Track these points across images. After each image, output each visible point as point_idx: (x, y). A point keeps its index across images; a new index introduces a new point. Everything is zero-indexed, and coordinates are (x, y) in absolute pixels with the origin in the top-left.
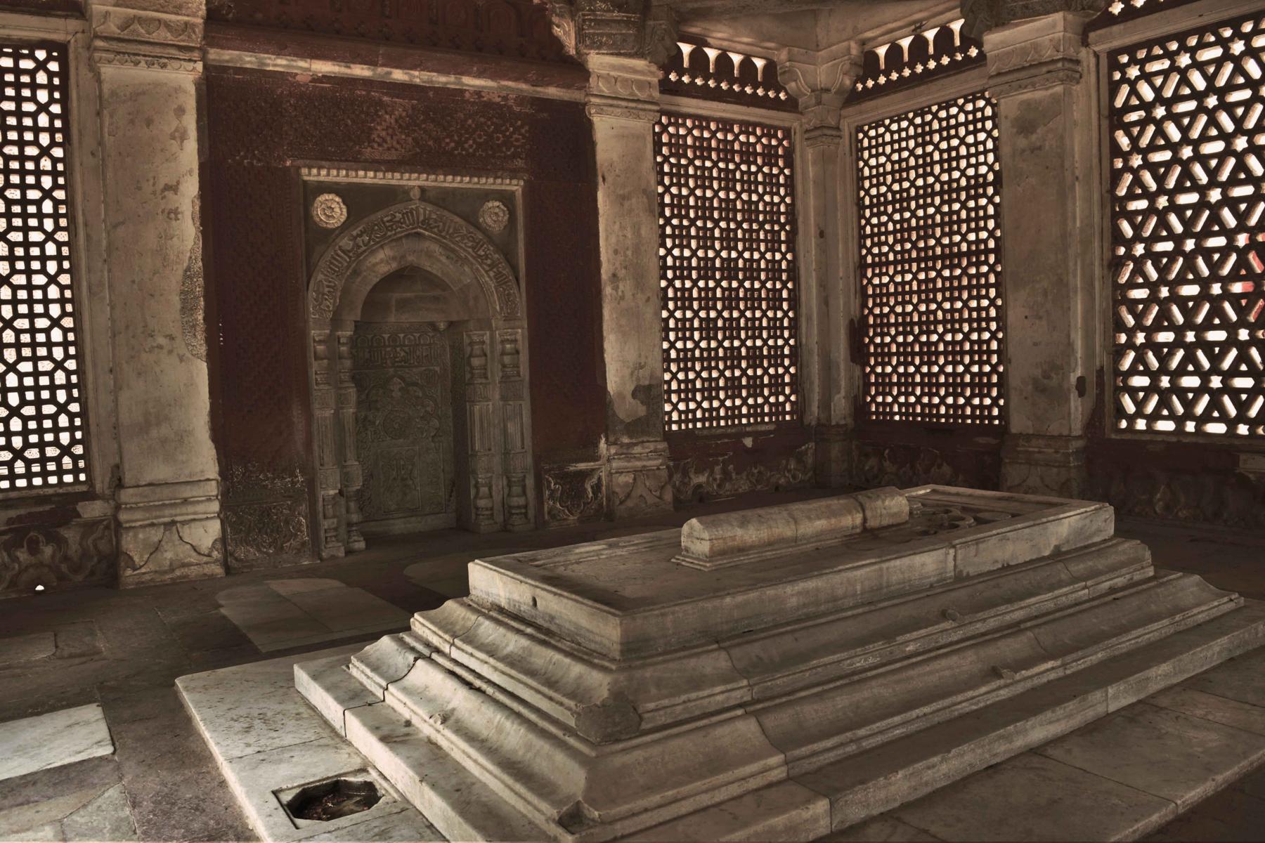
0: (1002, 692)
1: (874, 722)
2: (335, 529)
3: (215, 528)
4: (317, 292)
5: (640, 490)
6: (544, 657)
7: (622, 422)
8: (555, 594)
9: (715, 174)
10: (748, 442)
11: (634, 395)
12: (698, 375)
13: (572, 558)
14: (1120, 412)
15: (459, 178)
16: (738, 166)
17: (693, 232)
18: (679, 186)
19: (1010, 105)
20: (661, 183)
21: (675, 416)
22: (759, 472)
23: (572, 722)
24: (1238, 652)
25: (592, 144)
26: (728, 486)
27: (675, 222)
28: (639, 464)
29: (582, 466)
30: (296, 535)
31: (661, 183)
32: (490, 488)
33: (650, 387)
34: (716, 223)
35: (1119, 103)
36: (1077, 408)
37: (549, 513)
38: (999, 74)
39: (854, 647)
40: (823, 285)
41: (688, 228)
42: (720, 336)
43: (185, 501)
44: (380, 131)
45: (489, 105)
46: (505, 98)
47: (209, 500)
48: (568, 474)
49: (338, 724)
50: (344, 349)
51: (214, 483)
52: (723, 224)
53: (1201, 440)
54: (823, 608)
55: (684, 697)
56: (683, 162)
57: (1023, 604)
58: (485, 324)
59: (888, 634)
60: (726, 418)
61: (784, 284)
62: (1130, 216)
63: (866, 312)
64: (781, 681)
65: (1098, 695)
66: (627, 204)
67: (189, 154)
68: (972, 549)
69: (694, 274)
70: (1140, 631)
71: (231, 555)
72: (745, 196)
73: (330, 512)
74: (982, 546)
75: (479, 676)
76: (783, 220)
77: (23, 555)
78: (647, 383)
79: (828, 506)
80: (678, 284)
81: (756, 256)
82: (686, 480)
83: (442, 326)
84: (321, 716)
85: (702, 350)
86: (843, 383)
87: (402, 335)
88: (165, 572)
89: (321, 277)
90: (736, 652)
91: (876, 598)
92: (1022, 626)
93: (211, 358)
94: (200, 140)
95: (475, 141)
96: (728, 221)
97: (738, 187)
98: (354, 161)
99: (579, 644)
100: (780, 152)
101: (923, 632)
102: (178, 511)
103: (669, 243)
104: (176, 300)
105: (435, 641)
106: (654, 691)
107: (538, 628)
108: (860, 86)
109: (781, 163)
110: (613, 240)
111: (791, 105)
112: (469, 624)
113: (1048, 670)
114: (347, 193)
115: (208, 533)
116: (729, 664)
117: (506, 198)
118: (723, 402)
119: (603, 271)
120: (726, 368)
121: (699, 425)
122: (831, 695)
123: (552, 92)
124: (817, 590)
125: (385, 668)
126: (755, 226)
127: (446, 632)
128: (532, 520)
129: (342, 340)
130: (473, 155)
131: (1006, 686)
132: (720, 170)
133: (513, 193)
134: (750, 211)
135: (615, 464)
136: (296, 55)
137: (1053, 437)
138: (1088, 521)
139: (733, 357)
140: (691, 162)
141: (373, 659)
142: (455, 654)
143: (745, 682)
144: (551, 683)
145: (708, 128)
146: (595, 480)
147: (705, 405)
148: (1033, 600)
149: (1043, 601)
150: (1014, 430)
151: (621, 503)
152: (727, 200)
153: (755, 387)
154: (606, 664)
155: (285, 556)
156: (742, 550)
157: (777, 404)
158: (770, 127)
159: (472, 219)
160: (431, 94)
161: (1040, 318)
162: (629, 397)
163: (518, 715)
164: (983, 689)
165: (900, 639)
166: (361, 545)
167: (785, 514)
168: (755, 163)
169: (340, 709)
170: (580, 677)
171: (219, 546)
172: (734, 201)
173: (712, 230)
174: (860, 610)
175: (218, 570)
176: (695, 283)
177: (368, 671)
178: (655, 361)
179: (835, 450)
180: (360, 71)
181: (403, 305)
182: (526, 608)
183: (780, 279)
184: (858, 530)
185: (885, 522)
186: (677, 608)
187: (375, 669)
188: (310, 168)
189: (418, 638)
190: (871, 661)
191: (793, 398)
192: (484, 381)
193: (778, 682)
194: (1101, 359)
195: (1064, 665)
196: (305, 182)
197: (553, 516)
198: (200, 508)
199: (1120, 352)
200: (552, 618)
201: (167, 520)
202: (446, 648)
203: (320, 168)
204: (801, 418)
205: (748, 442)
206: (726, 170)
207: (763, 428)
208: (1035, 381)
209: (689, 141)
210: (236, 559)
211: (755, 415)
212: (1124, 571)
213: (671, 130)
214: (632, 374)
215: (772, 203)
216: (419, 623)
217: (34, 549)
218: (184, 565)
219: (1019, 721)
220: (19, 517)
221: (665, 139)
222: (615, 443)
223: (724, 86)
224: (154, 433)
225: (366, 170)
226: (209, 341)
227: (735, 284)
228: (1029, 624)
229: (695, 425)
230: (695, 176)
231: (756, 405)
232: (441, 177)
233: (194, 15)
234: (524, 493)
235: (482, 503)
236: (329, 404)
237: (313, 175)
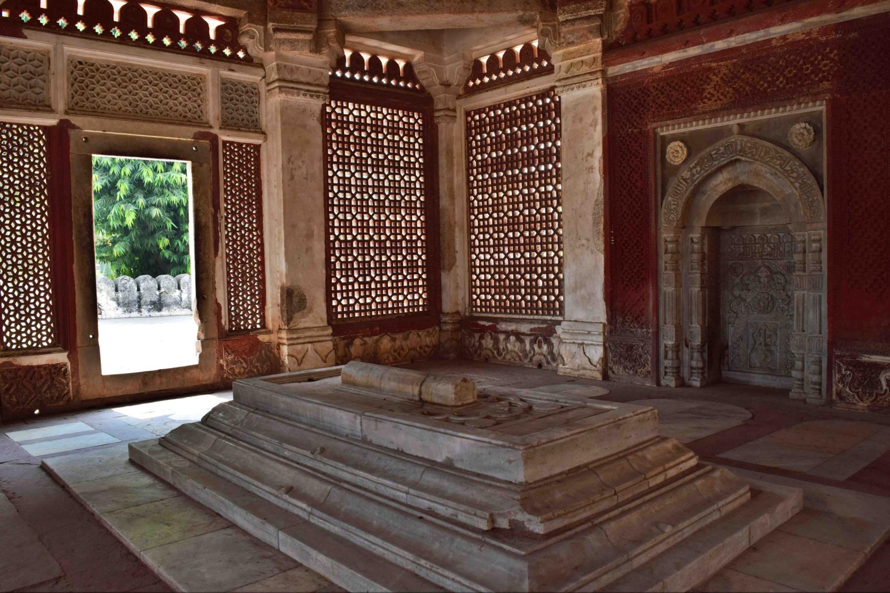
2: (702, 368)
3: (600, 350)
32: (803, 362)
37: (839, 394)
43: (589, 332)
44: (709, 89)
45: (795, 43)
46: (809, 34)
48: (863, 364)
50: (696, 246)
51: (601, 325)
57: (357, 472)
67: (598, 134)
73: (670, 353)
74: (380, 425)
77: (536, 347)
92: (342, 484)
93: (605, 250)
95: (784, 76)
115: (597, 354)
117: (813, 120)
123: (859, 12)
129: (695, 240)
130: (784, 88)
131: (277, 496)
133: (821, 112)
136: (653, 55)
148: (362, 473)
149: (346, 473)
165: (285, 445)
166: (697, 384)
175: (599, 377)
180: (693, 51)
185: (436, 400)
188: (662, 127)
190: (270, 448)
192: (801, 273)
195: (310, 513)
196: (663, 137)
198: (594, 338)
201: (580, 342)
203: (668, 126)
210: (613, 372)
217: (540, 347)
218: (584, 369)
220: (535, 329)
224: (578, 292)
226: (606, 242)
228: (346, 486)
233: (596, 52)
234: (820, 373)
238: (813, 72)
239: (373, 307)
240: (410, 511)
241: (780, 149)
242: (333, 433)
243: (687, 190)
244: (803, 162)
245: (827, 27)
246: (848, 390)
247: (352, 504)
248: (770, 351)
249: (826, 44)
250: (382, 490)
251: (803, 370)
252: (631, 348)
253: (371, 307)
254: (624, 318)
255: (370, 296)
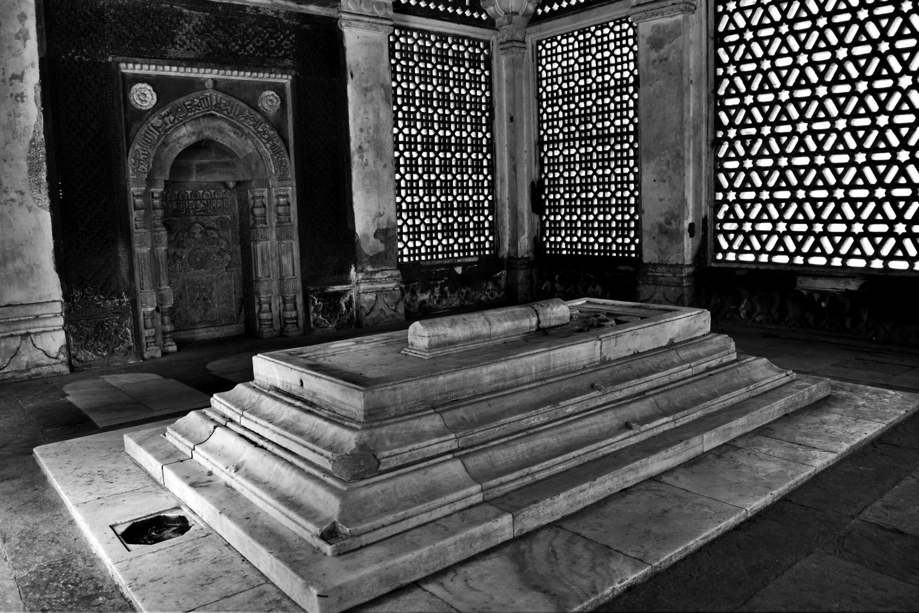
0: (632, 439)
1: (543, 461)
2: (154, 337)
4: (135, 158)
5: (380, 305)
6: (309, 422)
7: (367, 256)
8: (316, 377)
9: (434, 73)
10: (459, 270)
11: (375, 236)
12: (422, 221)
13: (329, 351)
14: (718, 248)
15: (242, 73)
16: (451, 68)
17: (418, 116)
18: (408, 82)
19: (646, 28)
20: (395, 79)
21: (406, 252)
22: (467, 292)
23: (329, 467)
24: (791, 410)
25: (343, 49)
26: (444, 302)
27: (405, 108)
28: (379, 286)
29: (338, 288)
30: (123, 342)
31: (395, 79)
32: (270, 305)
33: (386, 231)
34: (435, 109)
35: (721, 28)
36: (688, 245)
38: (638, 5)
39: (530, 410)
40: (513, 157)
41: (415, 113)
42: (438, 193)
44: (181, 36)
45: (265, 17)
46: (277, 13)
47: (56, 316)
49: (157, 475)
50: (157, 202)
51: (59, 304)
52: (440, 111)
53: (772, 268)
54: (508, 383)
55: (410, 447)
56: (411, 64)
58: (264, 183)
59: (554, 401)
60: (443, 253)
61: (485, 156)
62: (727, 109)
63: (543, 176)
64: (479, 434)
65: (696, 440)
66: (369, 95)
67: (31, 51)
68: (613, 342)
69: (419, 148)
70: (726, 396)
71: (74, 357)
72: (456, 91)
75: (262, 438)
76: (483, 108)
78: (385, 227)
79: (513, 312)
80: (407, 154)
81: (464, 134)
82: (414, 298)
83: (231, 185)
84: (146, 471)
85: (425, 203)
86: (526, 228)
87: (201, 192)
88: (23, 371)
89: (137, 147)
90: (447, 415)
91: (545, 377)
92: (647, 394)
93: (53, 209)
94: (39, 40)
96: (444, 108)
97: (451, 84)
98: (162, 58)
99: (334, 412)
100: (482, 58)
101: (578, 399)
102: (31, 325)
103: (400, 124)
104: (24, 165)
105: (229, 414)
106: (388, 443)
107: (305, 401)
108: (540, 11)
109: (482, 67)
110: (359, 121)
111: (490, 24)
112: (254, 400)
113: (664, 424)
114: (156, 83)
115: (55, 341)
116: (442, 423)
117: (279, 89)
118: (440, 241)
119: (352, 144)
120: (443, 216)
121: (423, 258)
122: (513, 443)
123: (313, 9)
124: (504, 370)
125: (192, 435)
126: (463, 113)
127: (237, 407)
128: (302, 328)
129: (155, 195)
130: (253, 55)
131: (635, 435)
132: (438, 71)
133: (283, 85)
134: (460, 101)
135: (363, 287)
137: (672, 266)
138: (692, 322)
139: (447, 208)
140: (417, 64)
141: (184, 428)
142: (244, 422)
143: (453, 436)
144: (315, 441)
145: (429, 39)
146: (347, 298)
147: (428, 243)
148: (654, 376)
149: (660, 377)
150: (645, 261)
151: (367, 315)
152: (443, 93)
153: (464, 230)
154: (354, 425)
155: (116, 358)
156: (451, 343)
157: (479, 242)
158: (474, 40)
159: (253, 104)
160: (220, 8)
161: (664, 181)
162: (372, 238)
163: (291, 464)
164: (619, 437)
165: (562, 404)
166: (174, 348)
167: (482, 318)
168: (464, 66)
169: (159, 465)
170: (335, 435)
171: (64, 350)
172: (448, 94)
173: (432, 115)
174: (534, 385)
175: (65, 369)
176: (420, 154)
177: (179, 437)
178: (391, 212)
179: (521, 275)
181: (201, 169)
182: (295, 388)
183: (481, 151)
184: (534, 329)
185: (554, 323)
186: (404, 385)
187: (185, 435)
188: (127, 63)
189: (216, 412)
190: (543, 419)
191: (491, 238)
192: (264, 226)
193: (477, 435)
194: (706, 210)
195: (674, 420)
196: (123, 74)
197: (317, 325)
199: (717, 205)
200: (315, 394)
202: (237, 418)
203: (135, 63)
204: (496, 253)
205: (459, 270)
206: (443, 71)
207: (470, 260)
208: (660, 226)
209: (415, 49)
210: (78, 360)
211: (464, 251)
212: (716, 356)
213: (402, 40)
214: (374, 220)
215: (476, 96)
216: (217, 401)
218: (38, 366)
219: (643, 458)
221: (397, 46)
222: (362, 271)
223: (441, 8)
224: (10, 266)
225: (171, 65)
226: (52, 195)
227: (449, 155)
228: (651, 392)
229: (420, 258)
230: (420, 75)
231: (464, 244)
232: (229, 72)
234: (295, 308)
235: (264, 316)
236: (146, 244)
237: (129, 69)
238: (277, 47)
239: (472, 246)
240: (701, 376)
241: (253, 112)
242: (569, 372)
243: (158, 140)
244: (273, 127)
245: (291, 13)
246: (320, 317)
247: (677, 397)
248: (208, 304)
249: (286, 27)
250: (675, 377)
251: (271, 311)
252: (101, 325)
253: (420, 250)
254: (83, 291)
255: (419, 239)
